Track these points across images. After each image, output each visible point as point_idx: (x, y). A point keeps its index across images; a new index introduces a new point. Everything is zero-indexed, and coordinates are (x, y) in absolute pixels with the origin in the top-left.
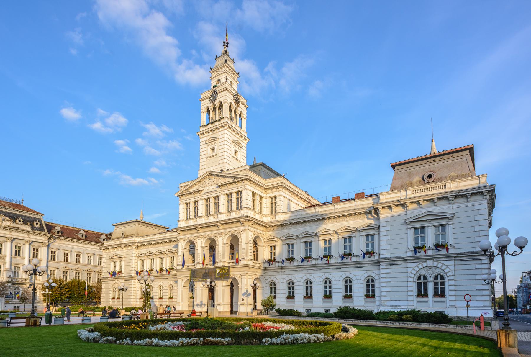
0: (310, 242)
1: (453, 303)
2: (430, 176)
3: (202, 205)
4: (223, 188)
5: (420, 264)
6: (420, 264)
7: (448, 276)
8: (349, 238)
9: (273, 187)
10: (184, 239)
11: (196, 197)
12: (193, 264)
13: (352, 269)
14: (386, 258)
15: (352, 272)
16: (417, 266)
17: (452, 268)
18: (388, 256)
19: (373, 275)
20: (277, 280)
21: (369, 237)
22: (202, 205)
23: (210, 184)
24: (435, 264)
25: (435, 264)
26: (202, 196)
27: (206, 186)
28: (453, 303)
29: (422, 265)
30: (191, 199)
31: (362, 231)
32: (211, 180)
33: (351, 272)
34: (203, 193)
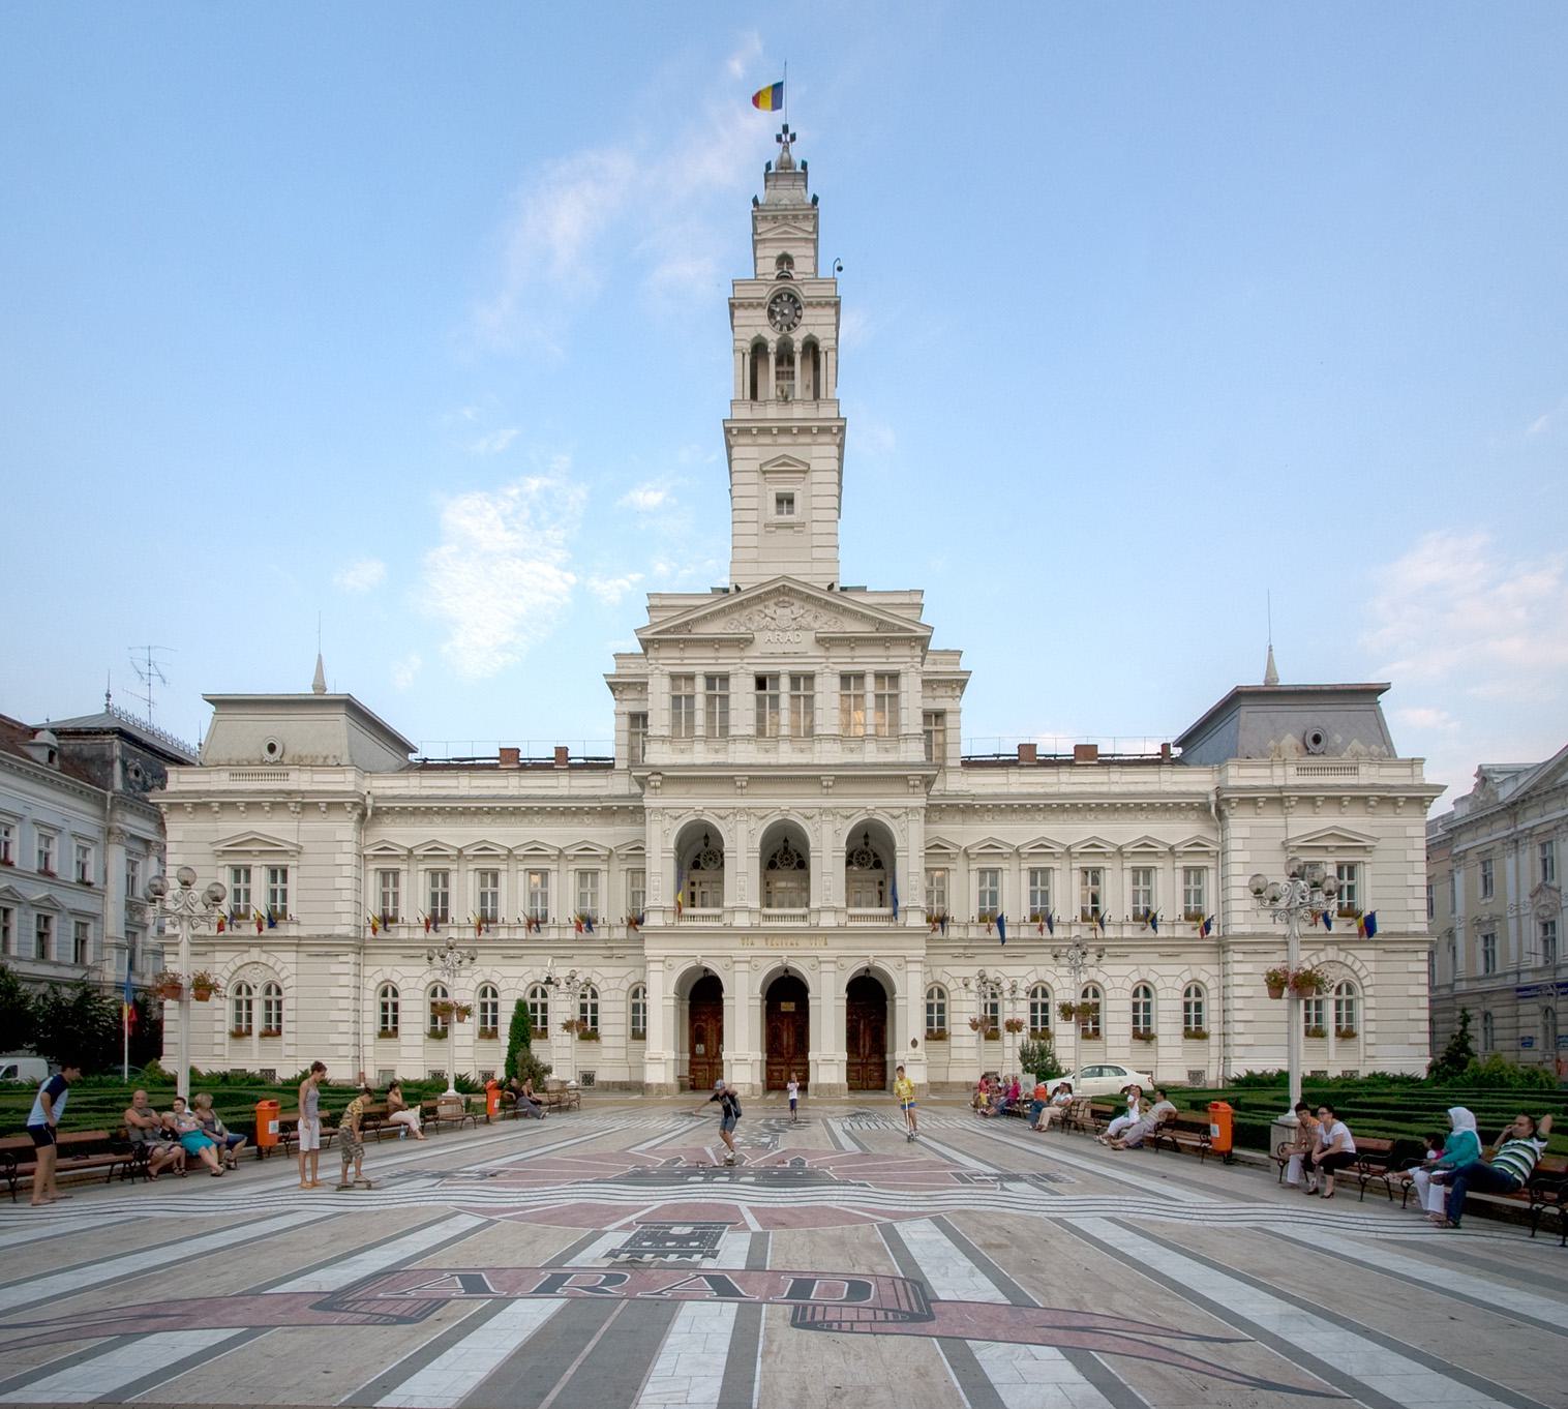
0: (1045, 871)
1: (1371, 1051)
2: (1317, 739)
3: (742, 693)
4: (835, 652)
5: (1313, 954)
6: (1313, 954)
7: (1363, 987)
8: (1144, 872)
9: (939, 681)
10: (675, 813)
11: (724, 662)
12: (717, 911)
13: (1154, 958)
14: (1243, 935)
15: (1153, 967)
16: (1307, 959)
17: (1371, 967)
18: (1247, 929)
19: (1203, 977)
20: (1159, 981)
21: (1194, 874)
22: (742, 693)
23: (784, 624)
24: (1342, 957)
25: (1342, 957)
26: (746, 661)
27: (767, 628)
28: (1371, 1051)
29: (1318, 957)
30: (700, 663)
31: (1181, 855)
32: (787, 611)
33: (1153, 967)
34: (752, 652)
